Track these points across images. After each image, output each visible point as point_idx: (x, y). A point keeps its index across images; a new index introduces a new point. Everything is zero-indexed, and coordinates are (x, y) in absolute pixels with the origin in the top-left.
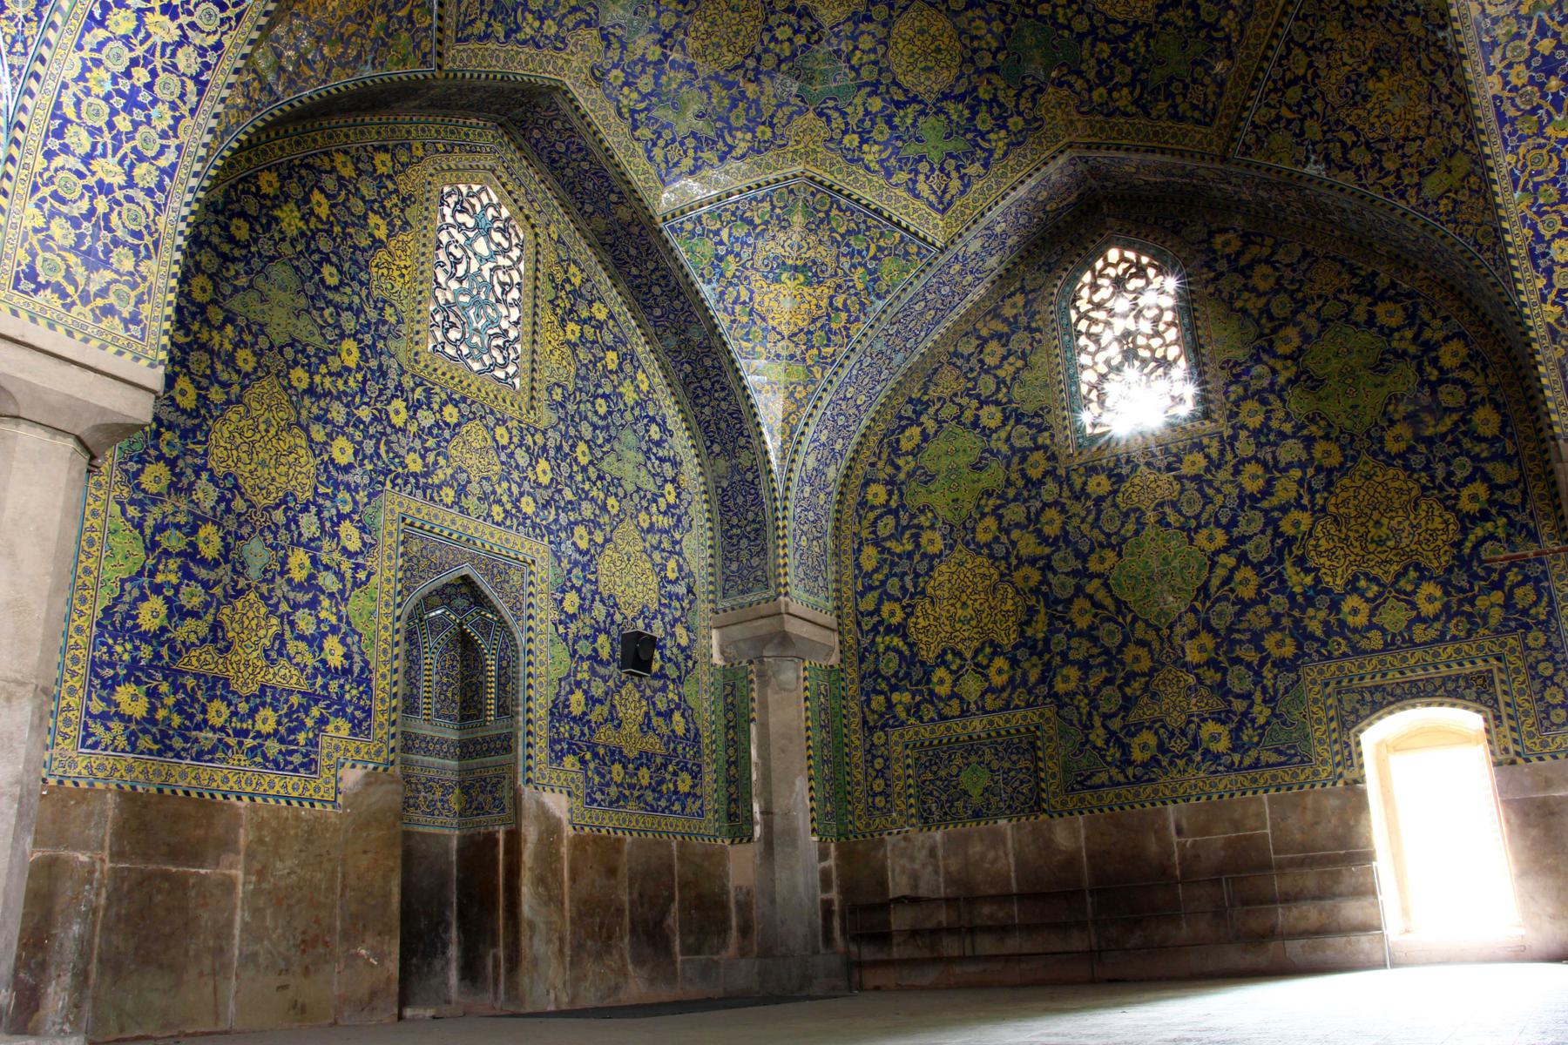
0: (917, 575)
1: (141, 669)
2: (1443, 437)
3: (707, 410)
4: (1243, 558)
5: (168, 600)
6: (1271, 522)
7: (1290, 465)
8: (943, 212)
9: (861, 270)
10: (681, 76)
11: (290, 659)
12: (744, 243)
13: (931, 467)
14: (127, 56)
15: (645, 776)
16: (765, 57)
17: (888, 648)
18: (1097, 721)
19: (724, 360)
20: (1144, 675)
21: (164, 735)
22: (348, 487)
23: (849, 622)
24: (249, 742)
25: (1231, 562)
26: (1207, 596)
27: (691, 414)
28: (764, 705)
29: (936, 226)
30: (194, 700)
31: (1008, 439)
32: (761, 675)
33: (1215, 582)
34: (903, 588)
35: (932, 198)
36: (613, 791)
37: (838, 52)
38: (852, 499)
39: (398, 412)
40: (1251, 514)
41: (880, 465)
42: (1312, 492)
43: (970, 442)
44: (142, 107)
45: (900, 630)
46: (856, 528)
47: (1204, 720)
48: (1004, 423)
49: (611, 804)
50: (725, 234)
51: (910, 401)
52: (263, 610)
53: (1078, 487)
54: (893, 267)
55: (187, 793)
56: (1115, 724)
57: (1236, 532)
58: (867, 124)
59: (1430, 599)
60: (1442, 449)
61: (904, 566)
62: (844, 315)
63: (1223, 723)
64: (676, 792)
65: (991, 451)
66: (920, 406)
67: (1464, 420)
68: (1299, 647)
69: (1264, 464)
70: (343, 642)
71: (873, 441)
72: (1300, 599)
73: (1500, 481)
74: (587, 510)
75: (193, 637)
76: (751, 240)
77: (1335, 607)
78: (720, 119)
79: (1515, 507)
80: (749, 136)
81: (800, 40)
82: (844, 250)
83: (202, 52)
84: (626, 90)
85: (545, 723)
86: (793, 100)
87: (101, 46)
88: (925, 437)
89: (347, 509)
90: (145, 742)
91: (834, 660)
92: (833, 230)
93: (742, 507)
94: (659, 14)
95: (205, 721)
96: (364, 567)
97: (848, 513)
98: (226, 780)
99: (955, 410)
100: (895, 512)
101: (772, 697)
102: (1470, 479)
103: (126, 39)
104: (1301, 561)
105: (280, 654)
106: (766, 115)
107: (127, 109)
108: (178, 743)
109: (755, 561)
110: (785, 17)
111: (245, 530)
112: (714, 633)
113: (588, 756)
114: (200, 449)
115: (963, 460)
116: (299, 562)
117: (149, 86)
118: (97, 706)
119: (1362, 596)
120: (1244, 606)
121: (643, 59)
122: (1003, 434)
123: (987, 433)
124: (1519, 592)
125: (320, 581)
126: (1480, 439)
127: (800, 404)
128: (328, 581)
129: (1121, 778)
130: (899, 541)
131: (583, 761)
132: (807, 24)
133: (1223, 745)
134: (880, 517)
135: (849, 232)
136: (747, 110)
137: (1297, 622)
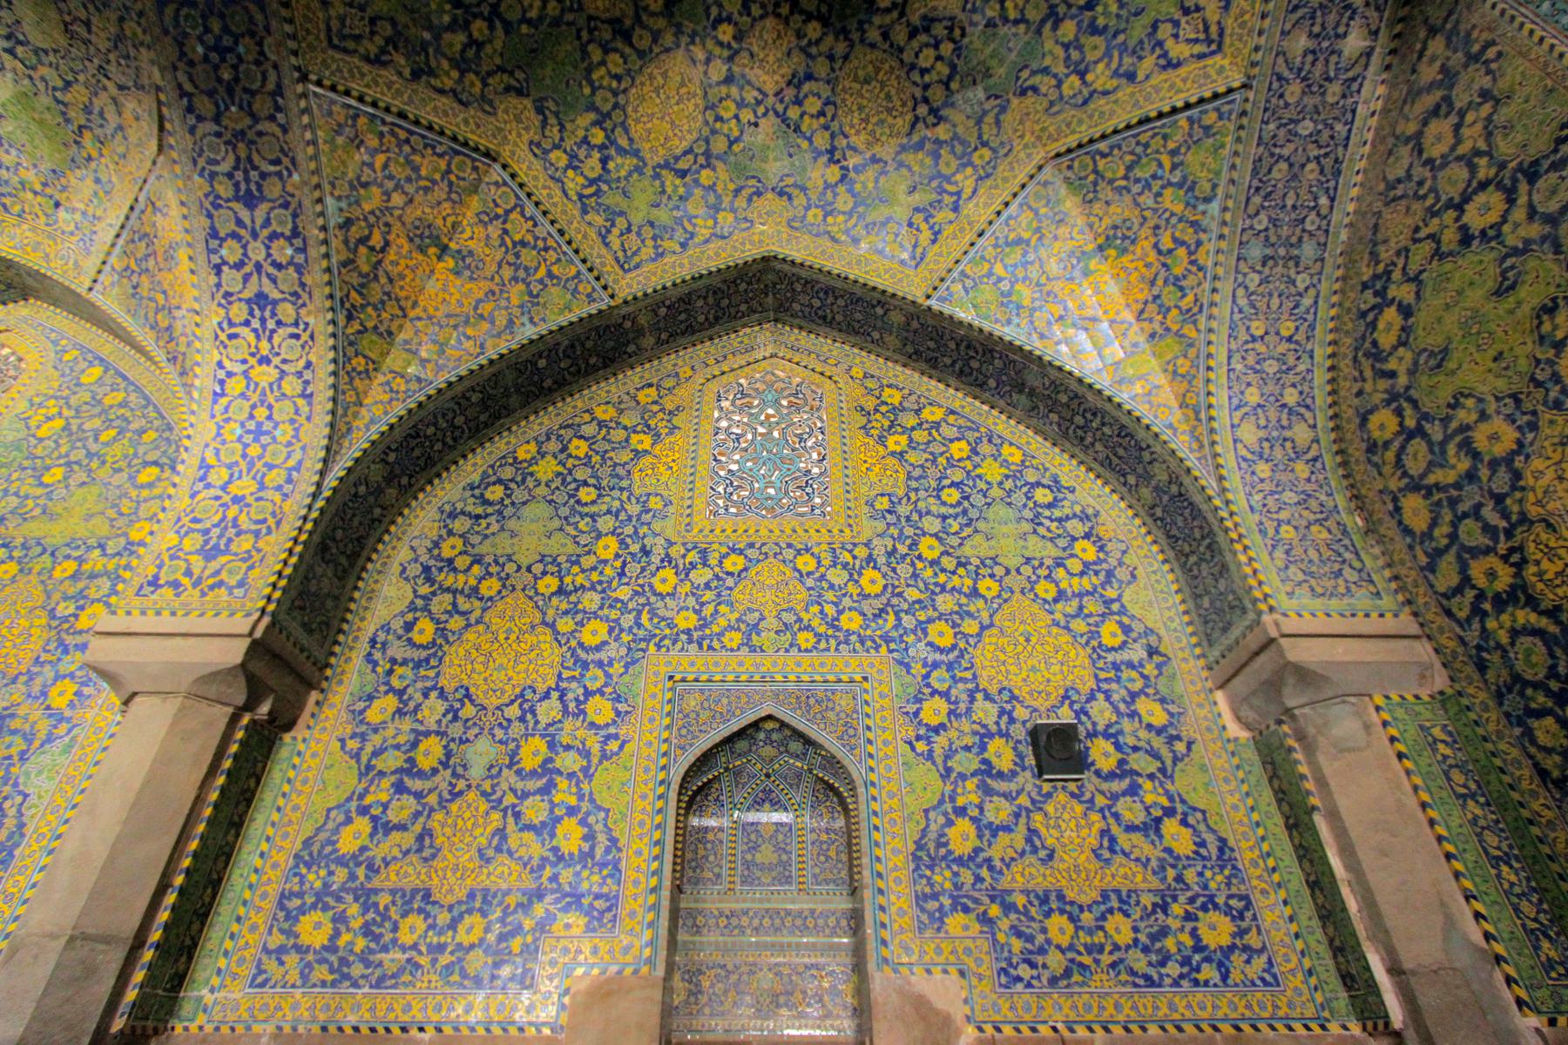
0: (1499, 499)
1: (331, 894)
3: (1099, 447)
5: (374, 819)
8: (1220, 48)
9: (1168, 192)
10: (871, 173)
11: (510, 854)
12: (1025, 264)
13: (1435, 341)
14: (247, 405)
15: (1120, 929)
16: (929, 93)
17: (1515, 633)
19: (1074, 385)
21: (344, 962)
22: (1131, 665)
23: (1432, 614)
24: (445, 959)
27: (1089, 460)
28: (1322, 782)
29: (1221, 70)
30: (385, 916)
31: (1532, 213)
32: (1301, 737)
34: (1487, 528)
35: (1198, 49)
36: (1055, 961)
37: (990, 24)
38: (1357, 451)
39: (666, 580)
41: (1368, 387)
43: (1480, 264)
44: (267, 433)
45: (1519, 595)
46: (1379, 485)
48: (1511, 201)
49: (1053, 981)
50: (999, 269)
51: (1365, 286)
52: (483, 807)
54: (1202, 155)
55: (356, 1029)
58: (1075, 55)
61: (1471, 496)
62: (1182, 252)
64: (1199, 947)
65: (1515, 252)
66: (1378, 285)
70: (583, 822)
71: (1346, 365)
74: (946, 603)
75: (396, 852)
76: (1031, 257)
78: (932, 179)
80: (969, 170)
81: (947, 49)
82: (1136, 188)
83: (299, 374)
84: (830, 220)
85: (904, 874)
86: (987, 106)
87: (227, 409)
88: (1406, 311)
89: (1138, 686)
90: (321, 973)
91: (1440, 681)
92: (1111, 182)
93: (1186, 527)
94: (810, 140)
95: (395, 941)
96: (616, 737)
97: (1360, 468)
98: (408, 1008)
99: (1427, 248)
100: (1419, 431)
101: (1328, 767)
103: (243, 395)
105: (498, 849)
106: (973, 141)
107: (256, 440)
108: (357, 970)
109: (1222, 585)
110: (915, 44)
111: (471, 734)
112: (1219, 696)
113: (994, 911)
114: (968, 675)
115: (1475, 296)
116: (533, 752)
117: (269, 418)
118: (276, 940)
121: (827, 186)
122: (1519, 214)
123: (1490, 235)
125: (558, 763)
127: (1189, 378)
128: (569, 761)
131: (985, 919)
132: (939, 30)
134: (1403, 448)
135: (1129, 168)
136: (953, 152)
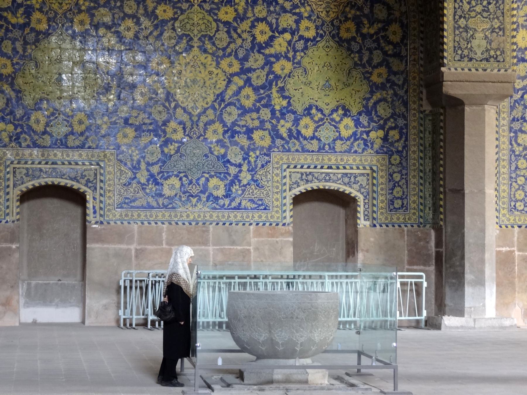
2: (371, 36)
4: (248, 82)
6: (268, 63)
7: (284, 31)
18: (143, 166)
20: (177, 142)
25: (241, 83)
26: (223, 100)
33: (230, 92)
40: (257, 55)
42: (295, 51)
47: (212, 177)
53: (150, 9)
56: (155, 169)
57: (247, 65)
59: (346, 127)
60: (369, 43)
63: (222, 180)
67: (384, 29)
68: (273, 142)
69: (270, 25)
72: (278, 114)
73: (395, 69)
77: (296, 122)
79: (398, 86)
102: (380, 65)
104: (282, 90)
119: (312, 118)
120: (245, 111)
124: (392, 133)
126: (390, 43)
129: (154, 204)
130: (14, 14)
133: (221, 192)
137: (274, 127)
